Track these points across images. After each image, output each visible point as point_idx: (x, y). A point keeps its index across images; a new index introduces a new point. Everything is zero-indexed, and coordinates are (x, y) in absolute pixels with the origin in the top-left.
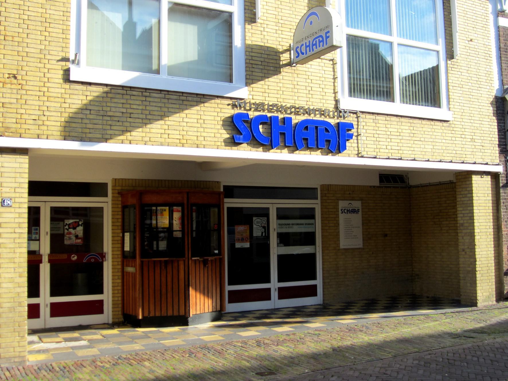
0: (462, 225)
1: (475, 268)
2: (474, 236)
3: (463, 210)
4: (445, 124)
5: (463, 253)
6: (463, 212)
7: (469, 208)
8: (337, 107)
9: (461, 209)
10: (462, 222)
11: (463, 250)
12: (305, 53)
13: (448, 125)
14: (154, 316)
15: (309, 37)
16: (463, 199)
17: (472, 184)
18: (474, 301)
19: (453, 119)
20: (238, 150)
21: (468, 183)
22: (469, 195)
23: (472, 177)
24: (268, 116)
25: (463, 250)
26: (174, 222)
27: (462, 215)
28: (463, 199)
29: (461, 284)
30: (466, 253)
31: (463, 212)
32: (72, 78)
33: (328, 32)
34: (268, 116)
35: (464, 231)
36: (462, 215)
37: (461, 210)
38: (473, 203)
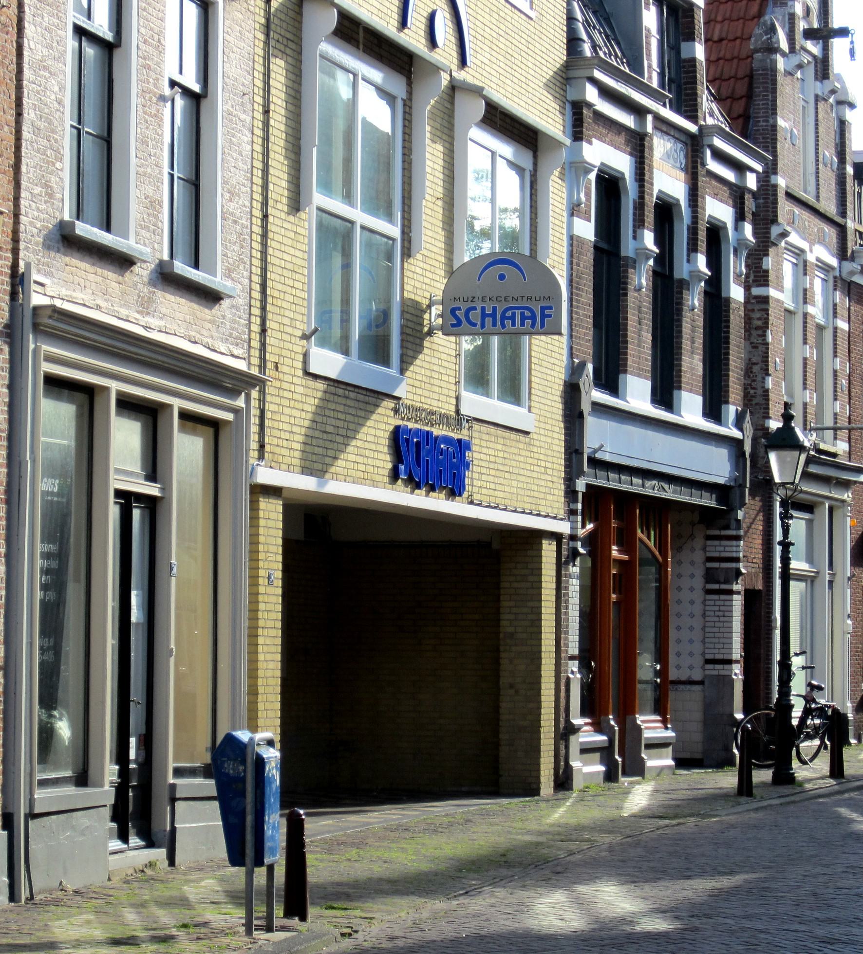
0: (512, 635)
1: (539, 721)
2: (540, 658)
3: (515, 607)
4: (521, 437)
5: (512, 692)
6: (514, 610)
7: (530, 604)
8: (458, 412)
9: (512, 604)
10: (511, 630)
11: (511, 686)
12: (479, 323)
13: (527, 440)
14: (216, 804)
15: (494, 299)
16: (515, 585)
17: (541, 556)
18: (534, 786)
19: (537, 430)
20: (392, 489)
21: (530, 553)
22: (531, 578)
23: (541, 544)
24: (409, 427)
25: (511, 686)
26: (652, 634)
27: (512, 617)
28: (515, 585)
29: (502, 754)
30: (517, 692)
31: (514, 610)
32: (312, 370)
33: (550, 308)
34: (409, 427)
35: (513, 648)
36: (512, 617)
37: (510, 607)
38: (540, 594)
